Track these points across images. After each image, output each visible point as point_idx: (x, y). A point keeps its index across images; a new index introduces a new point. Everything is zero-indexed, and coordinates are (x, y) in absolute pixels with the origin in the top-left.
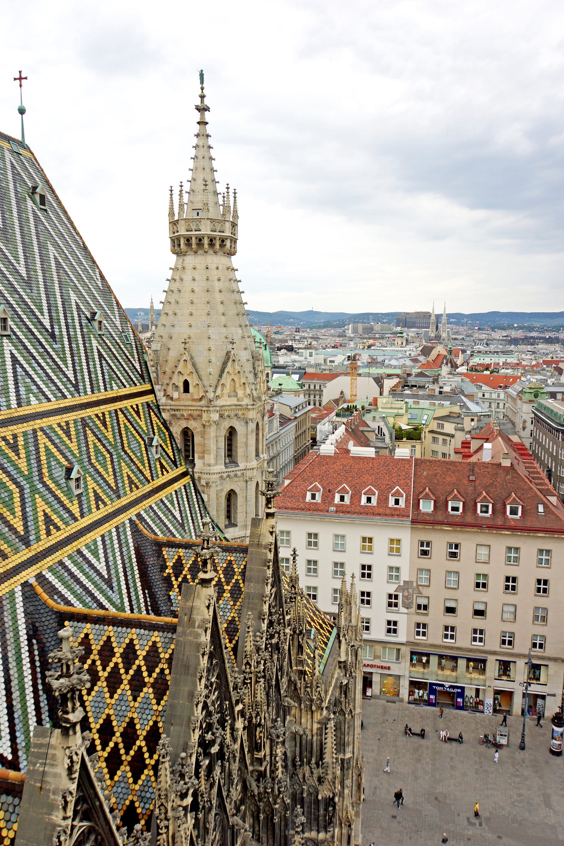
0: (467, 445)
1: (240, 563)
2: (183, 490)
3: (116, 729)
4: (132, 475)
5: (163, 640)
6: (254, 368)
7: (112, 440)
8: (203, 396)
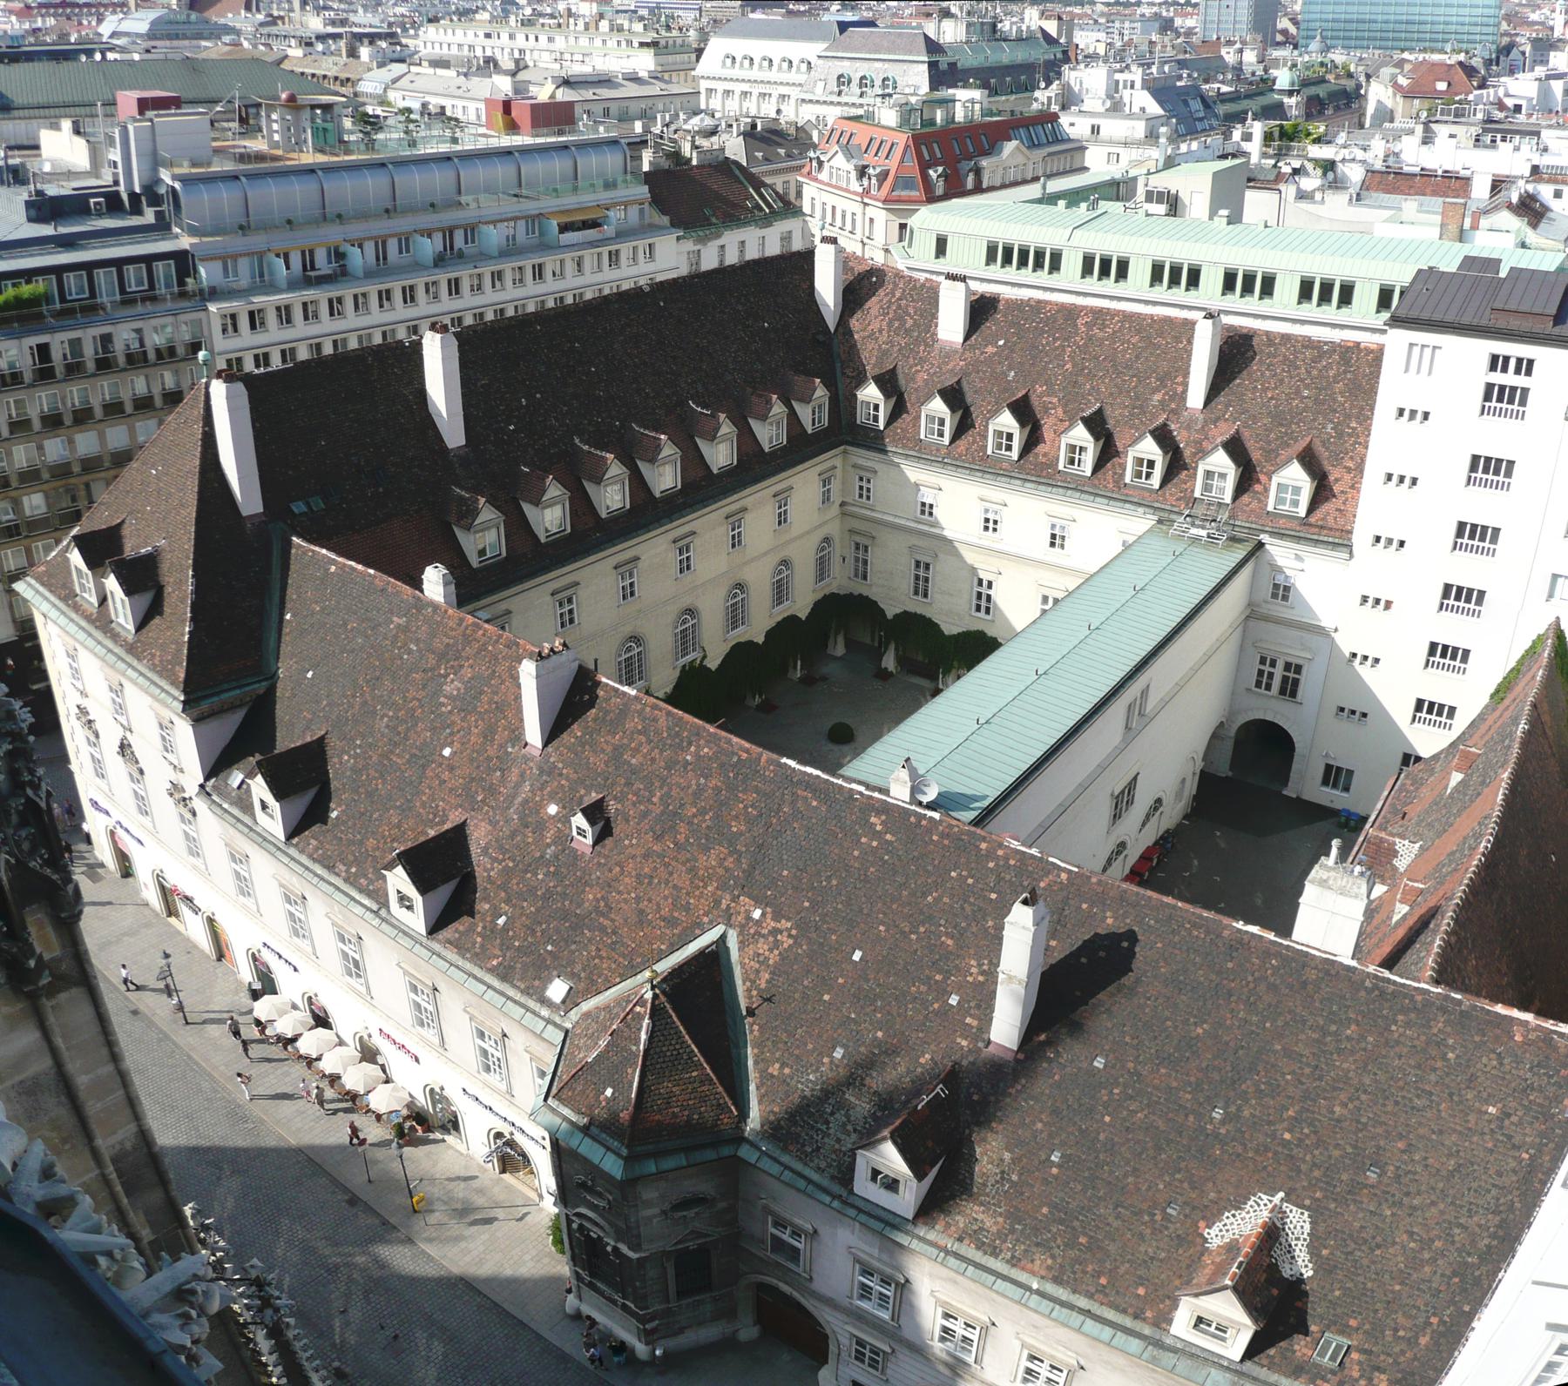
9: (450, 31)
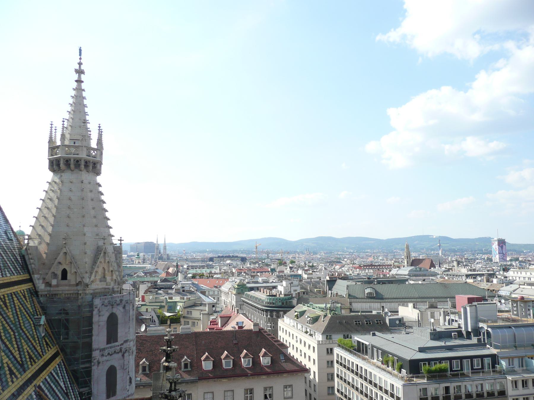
0: (215, 323)
2: (62, 364)
4: (30, 351)
6: (116, 259)
7: (12, 319)
8: (79, 282)
9: (519, 273)
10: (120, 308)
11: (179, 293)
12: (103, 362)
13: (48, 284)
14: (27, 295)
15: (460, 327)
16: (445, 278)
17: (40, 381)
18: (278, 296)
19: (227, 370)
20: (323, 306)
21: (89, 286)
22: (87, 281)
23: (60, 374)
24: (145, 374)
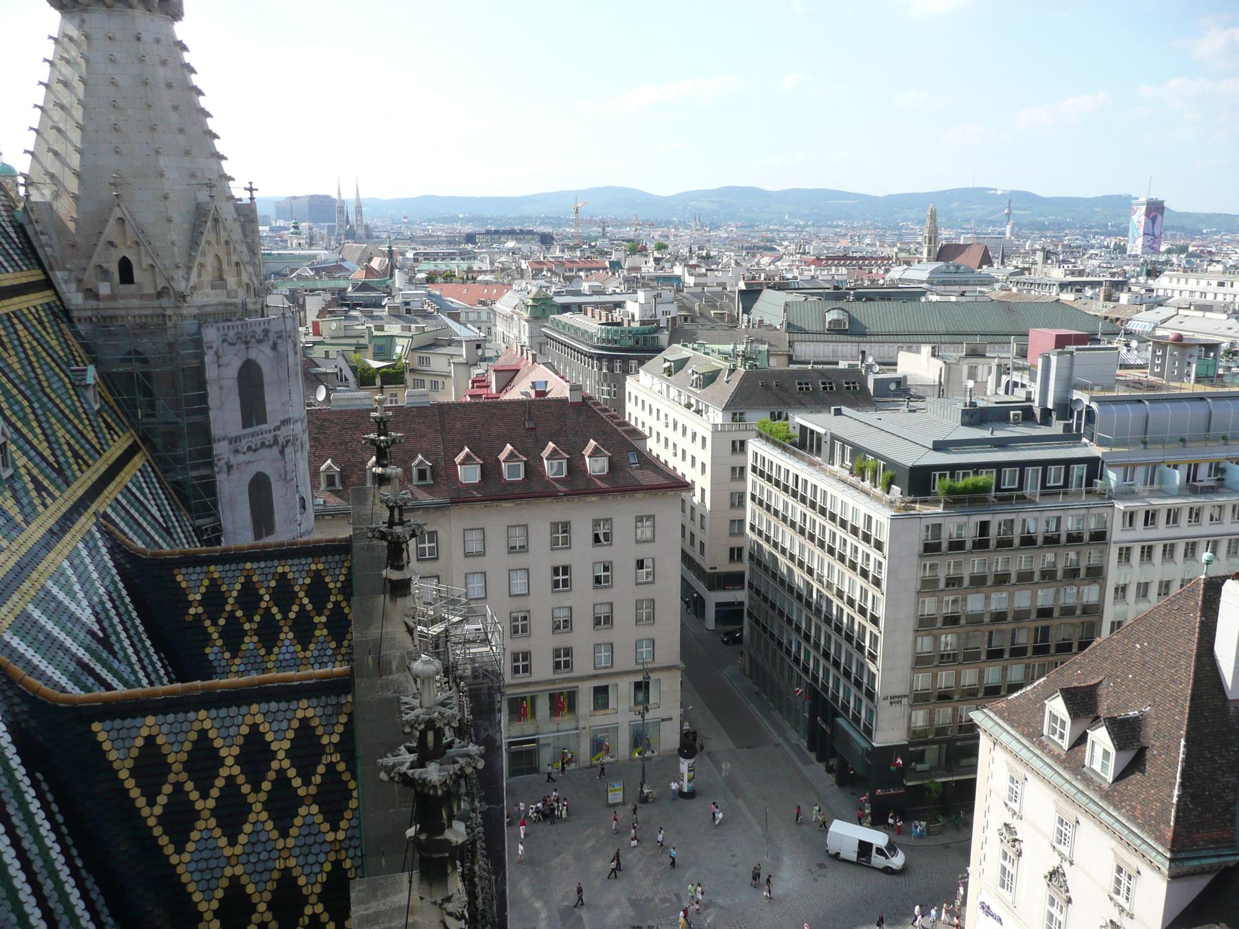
1: (337, 572)
2: (149, 469)
3: (255, 898)
4: (72, 442)
5: (319, 711)
6: (245, 236)
7: (20, 372)
8: (164, 288)
9: (1183, 281)
10: (266, 348)
11: (398, 317)
12: (238, 465)
13: (92, 294)
14: (45, 319)
15: (1029, 399)
16: (1010, 290)
17: (105, 505)
18: (626, 325)
19: (511, 483)
20: (728, 348)
21: (188, 299)
22: (181, 286)
23: (147, 491)
24: (332, 492)
